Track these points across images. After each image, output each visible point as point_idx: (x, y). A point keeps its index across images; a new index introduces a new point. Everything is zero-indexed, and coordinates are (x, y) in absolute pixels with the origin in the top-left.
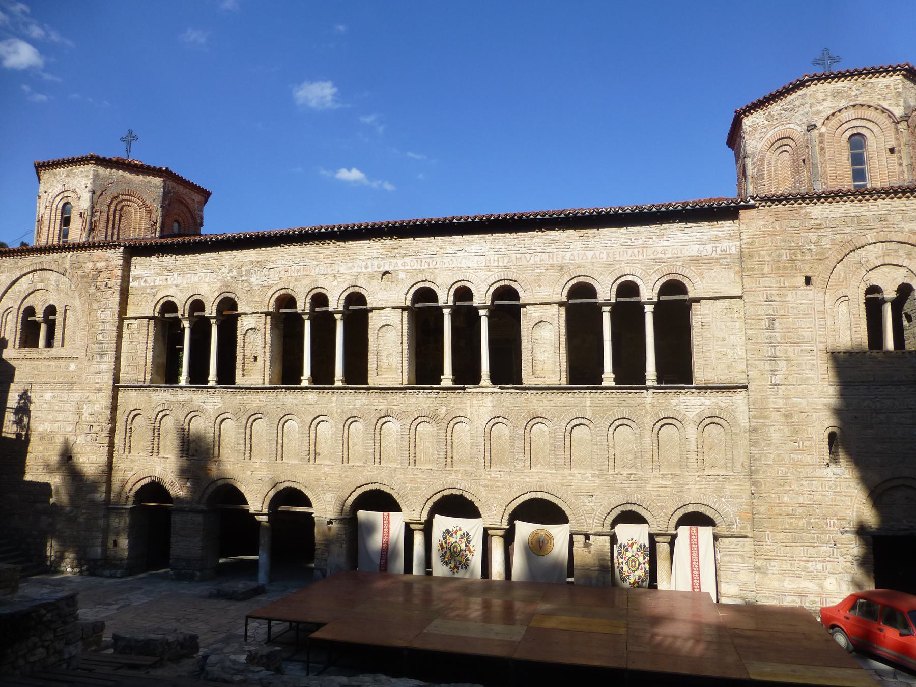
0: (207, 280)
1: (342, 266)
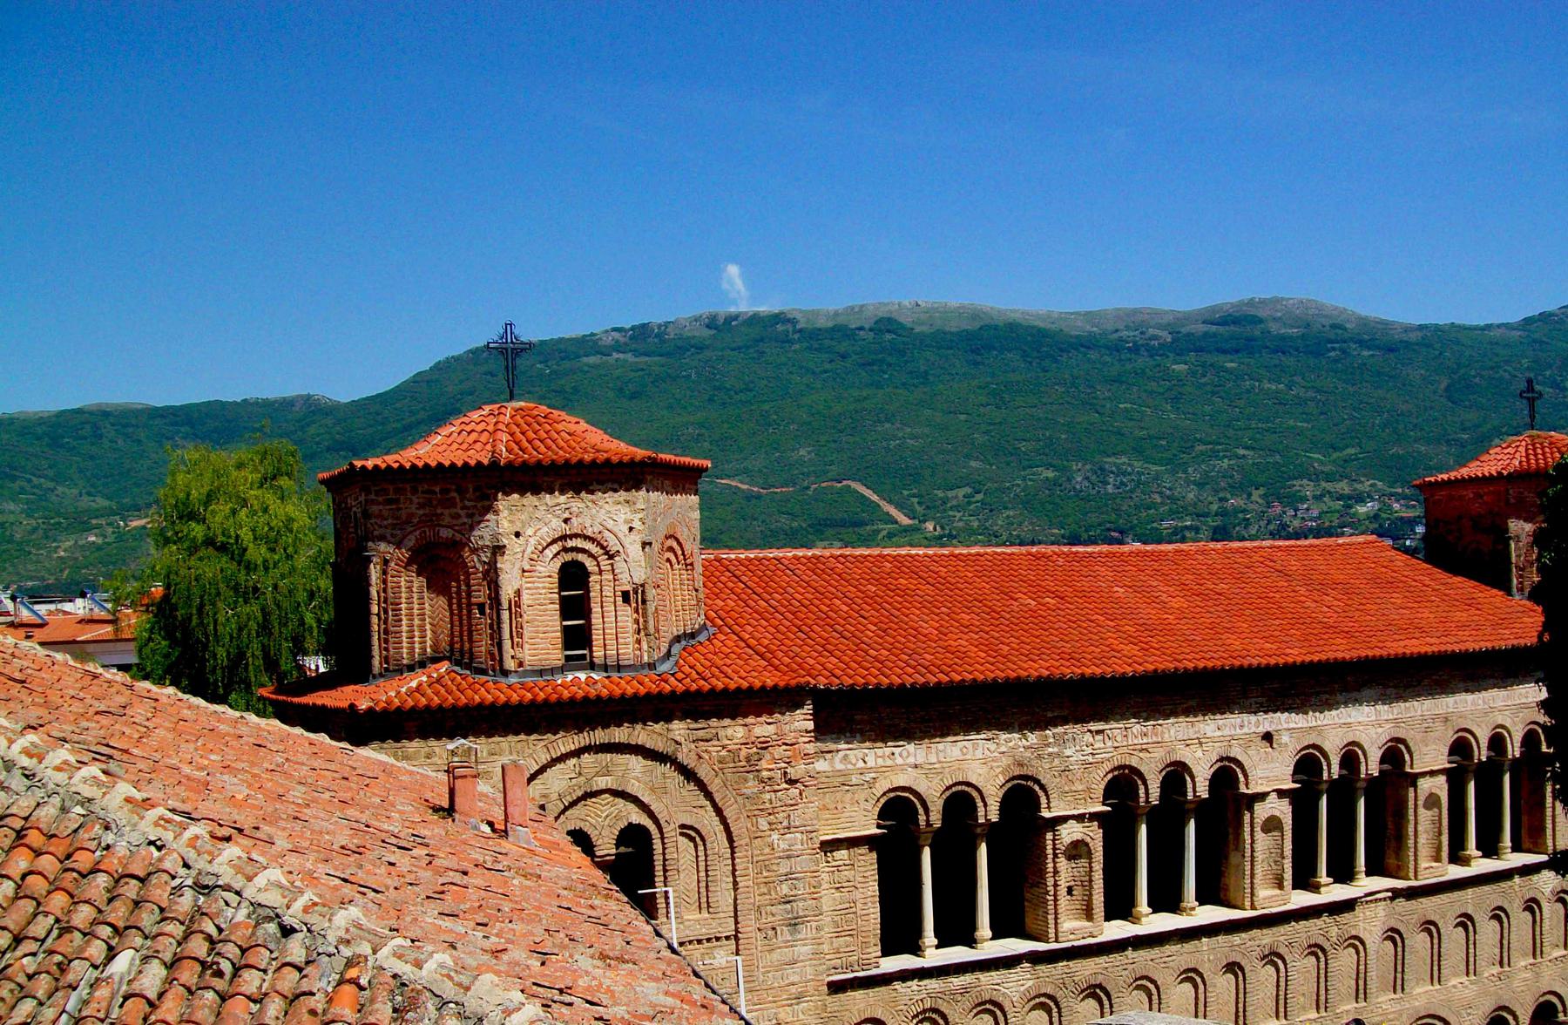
0: (979, 754)
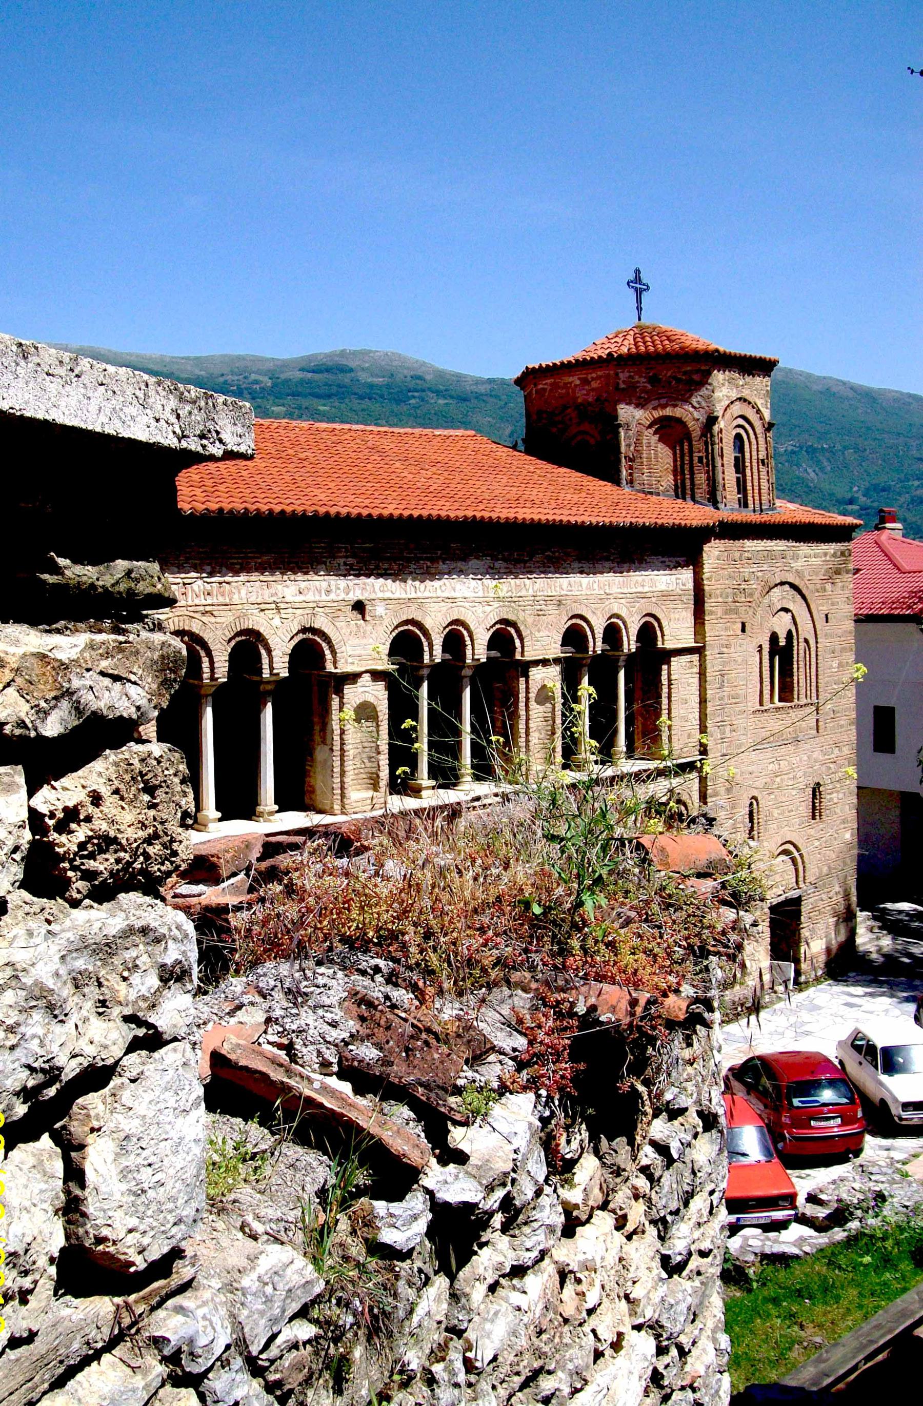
1: (287, 586)
